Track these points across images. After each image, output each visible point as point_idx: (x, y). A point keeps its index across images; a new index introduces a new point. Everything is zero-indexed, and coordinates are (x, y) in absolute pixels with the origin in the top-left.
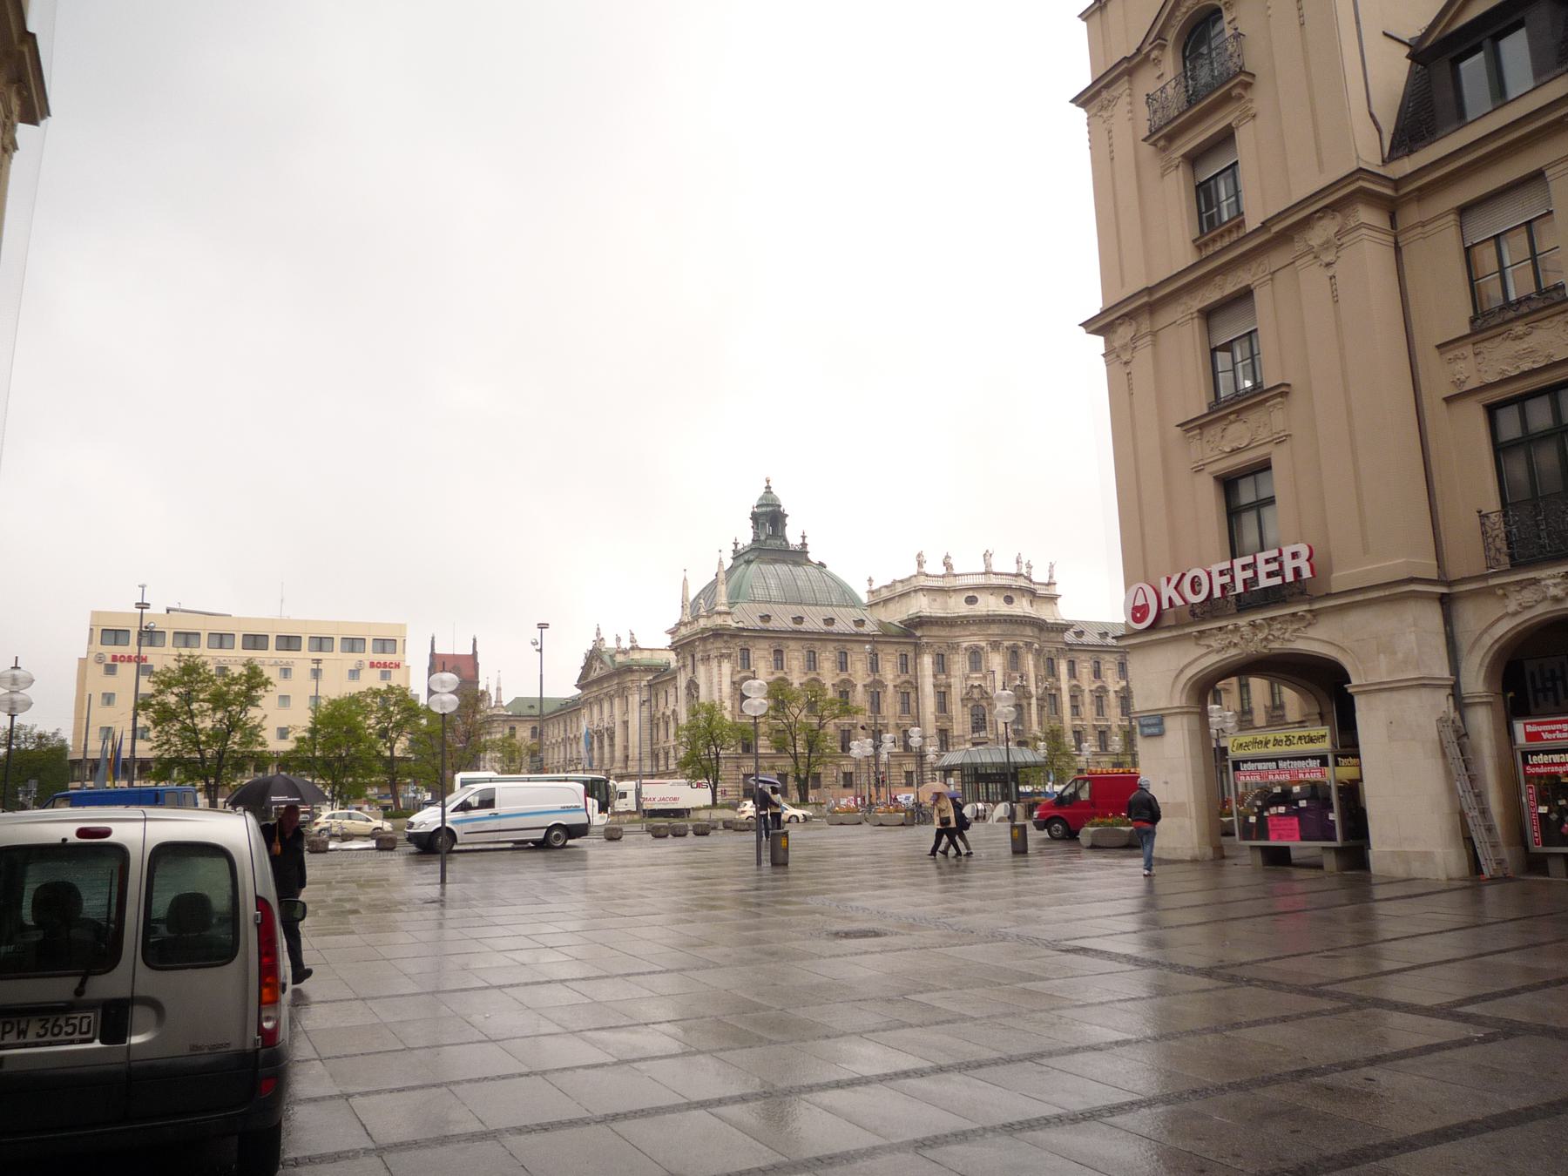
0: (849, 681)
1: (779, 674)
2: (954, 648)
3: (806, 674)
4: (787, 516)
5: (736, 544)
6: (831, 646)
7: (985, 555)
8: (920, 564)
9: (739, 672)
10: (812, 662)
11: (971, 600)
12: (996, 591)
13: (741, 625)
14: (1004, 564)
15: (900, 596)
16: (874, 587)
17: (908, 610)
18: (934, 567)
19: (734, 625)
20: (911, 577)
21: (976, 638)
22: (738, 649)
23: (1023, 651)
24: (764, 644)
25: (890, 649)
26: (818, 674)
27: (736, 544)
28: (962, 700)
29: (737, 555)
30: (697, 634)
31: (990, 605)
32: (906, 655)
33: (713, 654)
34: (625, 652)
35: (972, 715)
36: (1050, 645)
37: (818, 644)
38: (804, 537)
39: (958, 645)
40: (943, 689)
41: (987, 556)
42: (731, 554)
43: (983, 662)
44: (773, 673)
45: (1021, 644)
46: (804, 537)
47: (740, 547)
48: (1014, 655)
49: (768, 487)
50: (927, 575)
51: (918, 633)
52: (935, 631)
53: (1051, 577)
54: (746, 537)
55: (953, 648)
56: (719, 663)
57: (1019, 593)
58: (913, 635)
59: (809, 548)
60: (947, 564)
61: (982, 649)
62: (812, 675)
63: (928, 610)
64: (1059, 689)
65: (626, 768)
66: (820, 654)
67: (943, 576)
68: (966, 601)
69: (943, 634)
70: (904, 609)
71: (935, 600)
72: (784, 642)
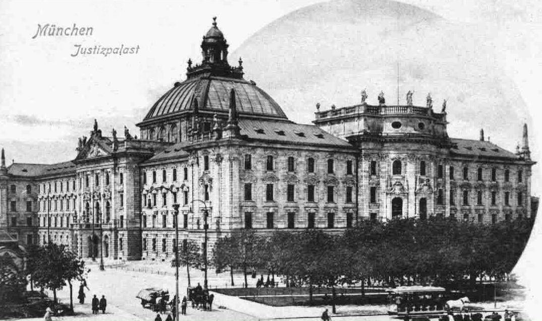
5: (190, 63)
7: (408, 94)
8: (364, 97)
16: (322, 110)
18: (373, 101)
27: (190, 63)
38: (240, 62)
40: (374, 186)
41: (410, 94)
42: (186, 71)
46: (240, 62)
47: (193, 65)
49: (215, 24)
53: (443, 110)
54: (198, 59)
59: (244, 71)
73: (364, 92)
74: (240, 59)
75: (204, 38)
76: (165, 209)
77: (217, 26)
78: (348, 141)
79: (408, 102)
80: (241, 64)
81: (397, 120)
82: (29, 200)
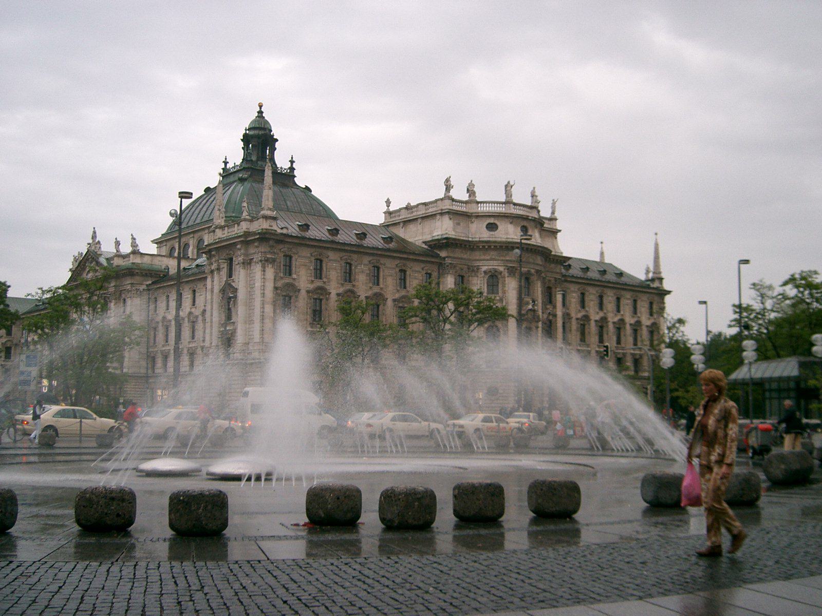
0: (380, 294)
1: (319, 283)
2: (474, 270)
3: (342, 285)
4: (277, 140)
5: (226, 163)
6: (366, 259)
7: (506, 186)
8: (448, 187)
9: (282, 278)
10: (348, 275)
11: (492, 227)
12: (515, 220)
13: (285, 231)
14: (521, 197)
15: (423, 218)
16: (392, 209)
17: (431, 233)
18: (460, 193)
19: (279, 231)
20: (436, 201)
21: (495, 263)
22: (281, 255)
23: (534, 278)
24: (306, 252)
25: (418, 267)
26: (354, 286)
27: (226, 163)
29: (226, 174)
30: (240, 236)
31: (509, 232)
32: (430, 275)
33: (257, 257)
34: (124, 257)
36: (549, 274)
37: (355, 256)
38: (292, 162)
39: (478, 268)
41: (508, 187)
43: (500, 286)
44: (312, 281)
45: (533, 271)
46: (292, 162)
48: (526, 281)
49: (260, 112)
50: (453, 200)
51: (443, 254)
52: (459, 253)
53: (553, 213)
54: (236, 157)
56: (264, 267)
57: (532, 224)
58: (438, 256)
59: (296, 173)
60: (471, 191)
61: (501, 273)
62: (348, 287)
63: (453, 233)
64: (555, 316)
66: (356, 267)
67: (466, 202)
68: (487, 228)
69: (465, 256)
70: (426, 230)
71: (458, 224)
72: (325, 251)
73: (447, 180)
74: (292, 158)
75: (246, 130)
77: (264, 115)
78: (426, 247)
79: (507, 197)
80: (292, 165)
81: (492, 220)
82: (8, 346)
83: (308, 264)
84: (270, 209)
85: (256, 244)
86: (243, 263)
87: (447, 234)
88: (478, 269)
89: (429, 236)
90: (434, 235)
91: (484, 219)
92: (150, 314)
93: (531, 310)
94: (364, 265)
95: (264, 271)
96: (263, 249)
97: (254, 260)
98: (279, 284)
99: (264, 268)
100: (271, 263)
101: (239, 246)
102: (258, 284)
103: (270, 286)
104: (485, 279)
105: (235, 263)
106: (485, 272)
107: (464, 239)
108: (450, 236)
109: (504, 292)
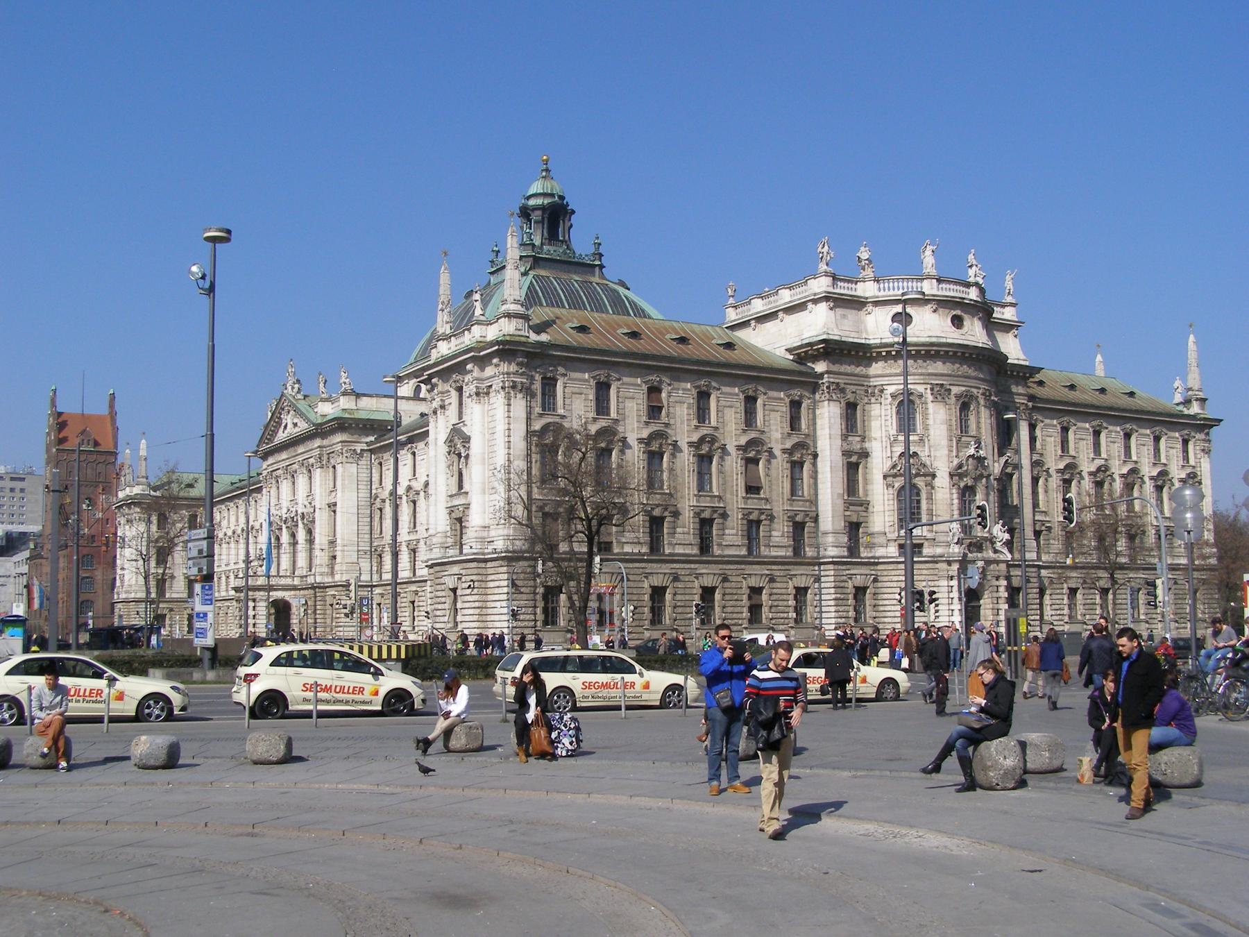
28: (885, 477)
35: (899, 501)
40: (854, 459)
51: (820, 367)
55: (873, 395)
64: (1017, 467)
65: (332, 574)
71: (844, 316)
76: (413, 537)
78: (791, 357)
83: (585, 391)
84: (516, 302)
85: (495, 361)
86: (478, 394)
87: (824, 333)
88: (882, 391)
89: (797, 339)
90: (804, 337)
91: (888, 308)
92: (373, 487)
93: (972, 456)
94: (683, 389)
95: (509, 405)
96: (504, 367)
97: (493, 387)
98: (537, 426)
99: (509, 399)
100: (521, 391)
101: (469, 367)
102: (501, 427)
103: (519, 430)
104: (894, 407)
105: (465, 395)
106: (893, 396)
107: (856, 341)
108: (831, 337)
109: (926, 427)
